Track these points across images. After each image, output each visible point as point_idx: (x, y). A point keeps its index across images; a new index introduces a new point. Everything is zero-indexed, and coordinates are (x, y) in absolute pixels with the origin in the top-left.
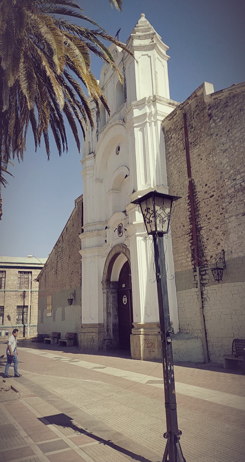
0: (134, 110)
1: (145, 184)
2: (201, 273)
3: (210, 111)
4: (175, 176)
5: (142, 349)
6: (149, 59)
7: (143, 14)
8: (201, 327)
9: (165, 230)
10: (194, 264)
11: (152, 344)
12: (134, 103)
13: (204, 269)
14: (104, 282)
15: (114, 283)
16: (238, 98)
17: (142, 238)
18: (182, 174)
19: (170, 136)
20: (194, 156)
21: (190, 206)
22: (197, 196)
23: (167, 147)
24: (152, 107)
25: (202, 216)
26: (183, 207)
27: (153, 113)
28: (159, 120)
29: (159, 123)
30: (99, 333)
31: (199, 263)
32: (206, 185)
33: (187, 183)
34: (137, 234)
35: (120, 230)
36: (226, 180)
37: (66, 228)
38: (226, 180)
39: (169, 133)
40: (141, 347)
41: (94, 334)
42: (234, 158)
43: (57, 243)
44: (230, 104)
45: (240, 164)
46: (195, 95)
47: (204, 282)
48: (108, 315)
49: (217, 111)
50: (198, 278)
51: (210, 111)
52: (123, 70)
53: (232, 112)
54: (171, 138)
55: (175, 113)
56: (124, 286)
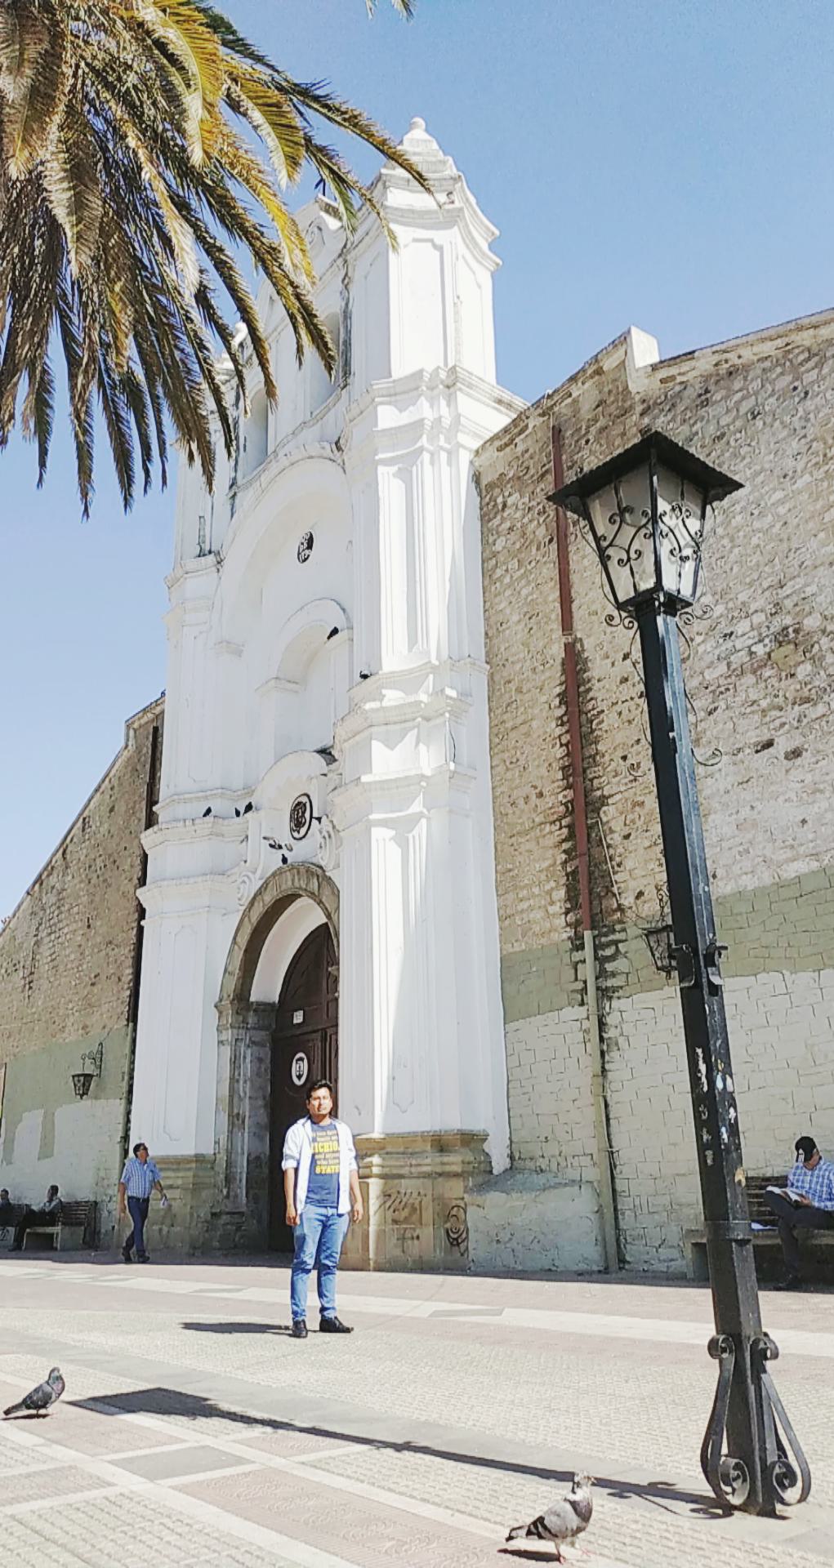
0: (380, 409)
1: (410, 650)
2: (600, 953)
3: (646, 420)
4: (515, 630)
5: (372, 1229)
6: (437, 253)
7: (419, 121)
8: (593, 1146)
9: (686, 592)
10: (576, 925)
11: (414, 1209)
12: (380, 385)
13: (611, 937)
14: (226, 1002)
15: (263, 1008)
16: (745, 379)
17: (393, 833)
18: (538, 623)
19: (500, 500)
21: (564, 729)
22: (591, 695)
23: (487, 535)
24: (443, 403)
25: (607, 758)
26: (541, 732)
27: (446, 422)
28: (465, 448)
29: (465, 458)
30: (196, 1188)
31: (592, 917)
32: (626, 657)
33: (557, 651)
34: (371, 817)
35: (300, 817)
36: (699, 639)
37: (84, 821)
38: (699, 639)
39: (497, 490)
40: (372, 1221)
41: (176, 1193)
42: (727, 568)
43: (40, 876)
44: (717, 397)
45: (750, 585)
46: (594, 369)
47: (610, 983)
48: (232, 1124)
49: (673, 419)
50: (588, 971)
51: (646, 420)
52: (341, 286)
53: (723, 423)
54: (505, 505)
55: (522, 425)
56: (298, 1018)
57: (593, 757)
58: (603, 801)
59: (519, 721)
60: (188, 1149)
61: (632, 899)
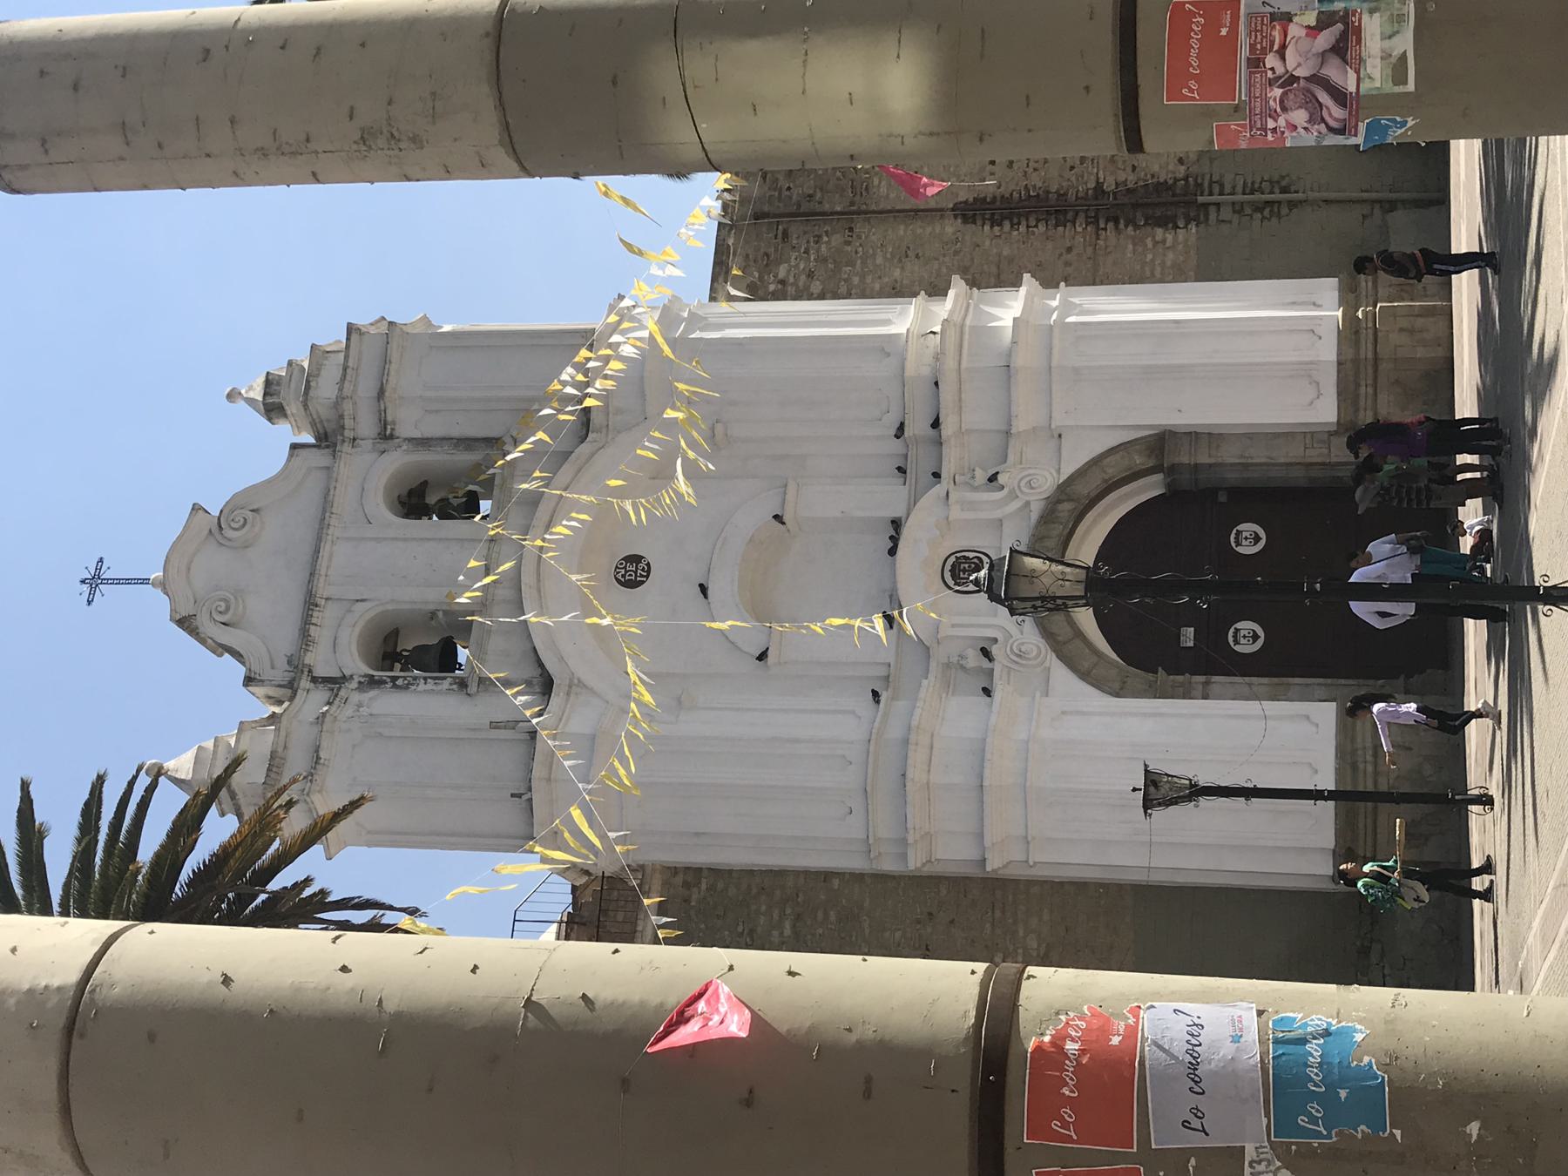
13: (1206, 184)
20: (892, 196)
21: (1024, 223)
33: (950, 227)
54: (782, 282)
57: (1060, 195)
58: (1099, 185)
59: (994, 269)
61: (1182, 168)
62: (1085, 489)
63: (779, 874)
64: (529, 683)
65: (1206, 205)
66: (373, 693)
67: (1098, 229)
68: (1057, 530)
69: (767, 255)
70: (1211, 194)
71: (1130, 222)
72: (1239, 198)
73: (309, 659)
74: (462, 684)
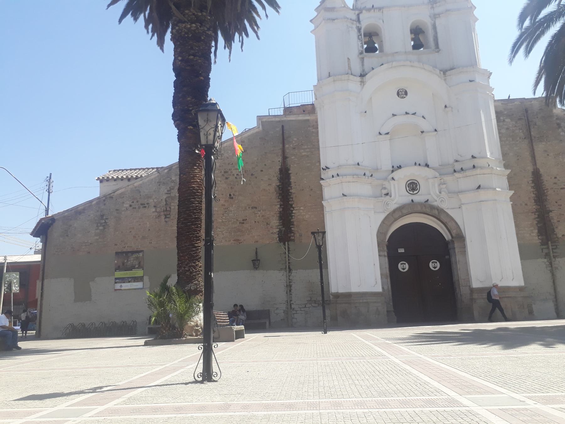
33: (530, 168)
47: (555, 254)
54: (504, 121)
58: (551, 211)
60: (379, 289)
61: (560, 236)
62: (443, 217)
63: (318, 149)
64: (363, 71)
65: (547, 244)
66: (356, 30)
67: (535, 213)
68: (428, 210)
69: (513, 114)
70: (552, 246)
71: (539, 222)
72: (552, 255)
73: (364, 12)
74: (361, 53)
